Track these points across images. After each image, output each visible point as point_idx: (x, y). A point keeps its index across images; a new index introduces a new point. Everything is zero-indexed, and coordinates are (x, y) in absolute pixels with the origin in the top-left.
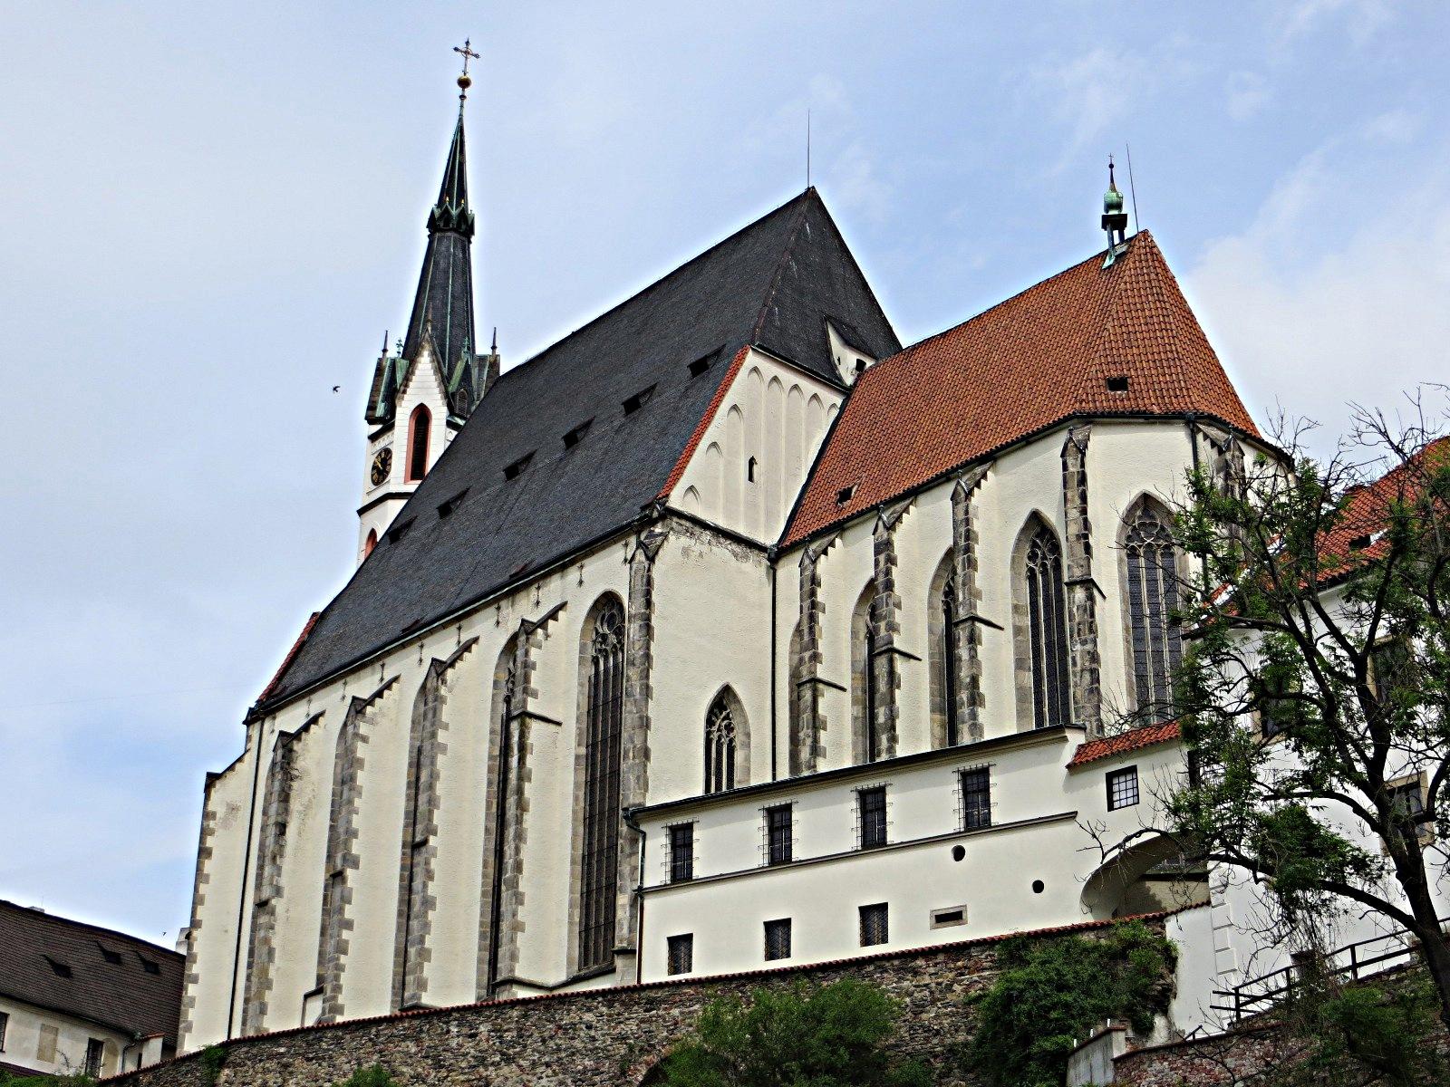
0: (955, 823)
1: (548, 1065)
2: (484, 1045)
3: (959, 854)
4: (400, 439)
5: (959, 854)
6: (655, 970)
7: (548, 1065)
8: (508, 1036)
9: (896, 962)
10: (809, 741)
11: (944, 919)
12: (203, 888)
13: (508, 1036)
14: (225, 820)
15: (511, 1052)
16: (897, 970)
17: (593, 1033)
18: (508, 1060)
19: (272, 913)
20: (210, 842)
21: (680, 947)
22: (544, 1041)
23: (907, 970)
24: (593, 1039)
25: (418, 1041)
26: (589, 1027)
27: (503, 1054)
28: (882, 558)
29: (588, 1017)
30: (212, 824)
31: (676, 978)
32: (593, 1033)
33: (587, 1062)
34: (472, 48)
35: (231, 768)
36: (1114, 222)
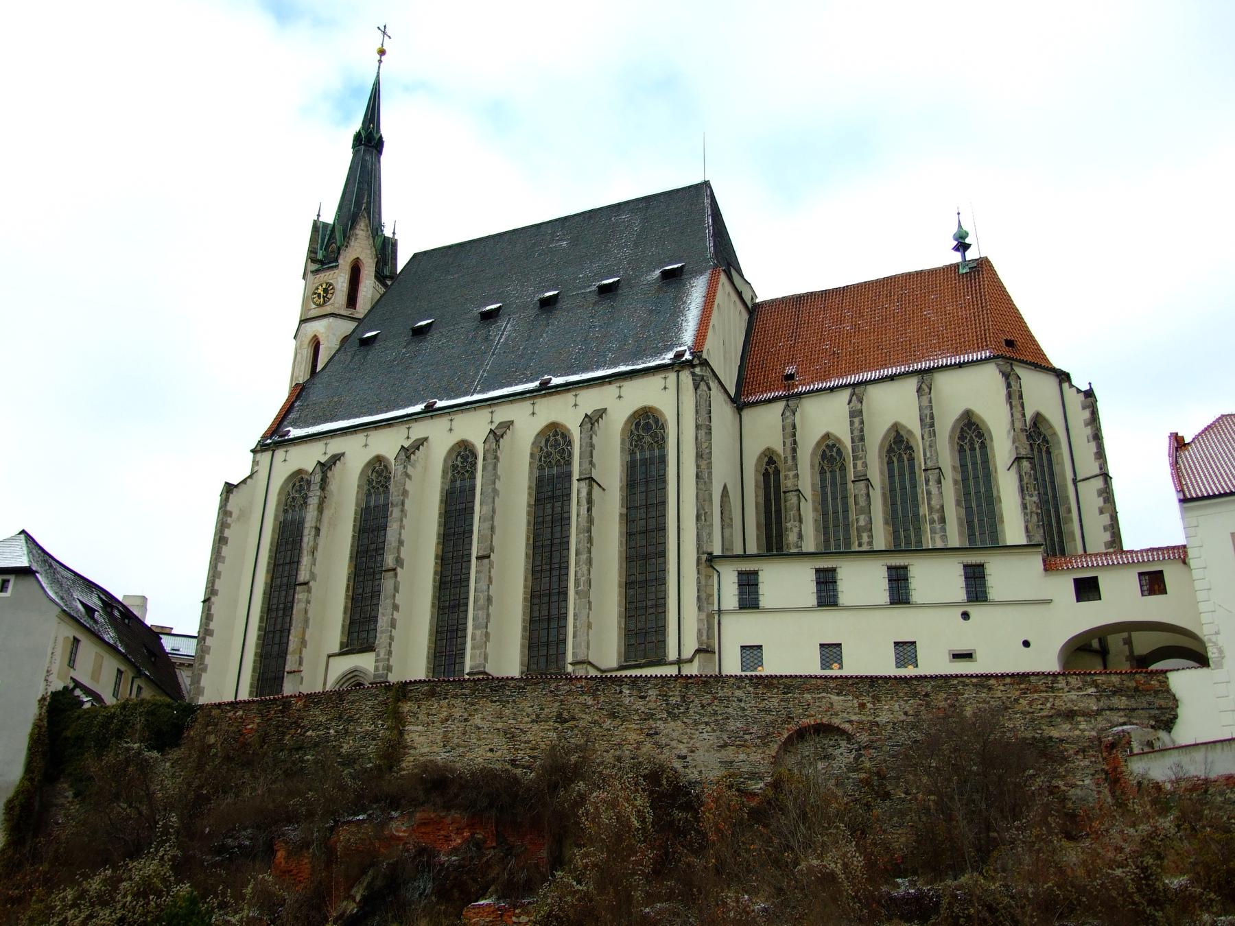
0: (960, 594)
1: (707, 723)
2: (652, 705)
3: (966, 616)
4: (340, 279)
5: (966, 616)
6: (732, 665)
7: (707, 723)
8: (673, 700)
9: (974, 680)
10: (796, 530)
11: (957, 656)
12: (220, 567)
13: (673, 700)
14: (238, 519)
15: (676, 711)
16: (975, 685)
17: (743, 705)
18: (675, 718)
19: (309, 591)
20: (227, 533)
21: (752, 653)
22: (703, 707)
23: (984, 687)
24: (743, 709)
25: (595, 697)
26: (740, 701)
27: (669, 713)
28: (857, 420)
29: (738, 693)
30: (229, 520)
31: (743, 674)
32: (743, 705)
33: (738, 724)
34: (388, 31)
35: (244, 481)
36: (962, 246)
